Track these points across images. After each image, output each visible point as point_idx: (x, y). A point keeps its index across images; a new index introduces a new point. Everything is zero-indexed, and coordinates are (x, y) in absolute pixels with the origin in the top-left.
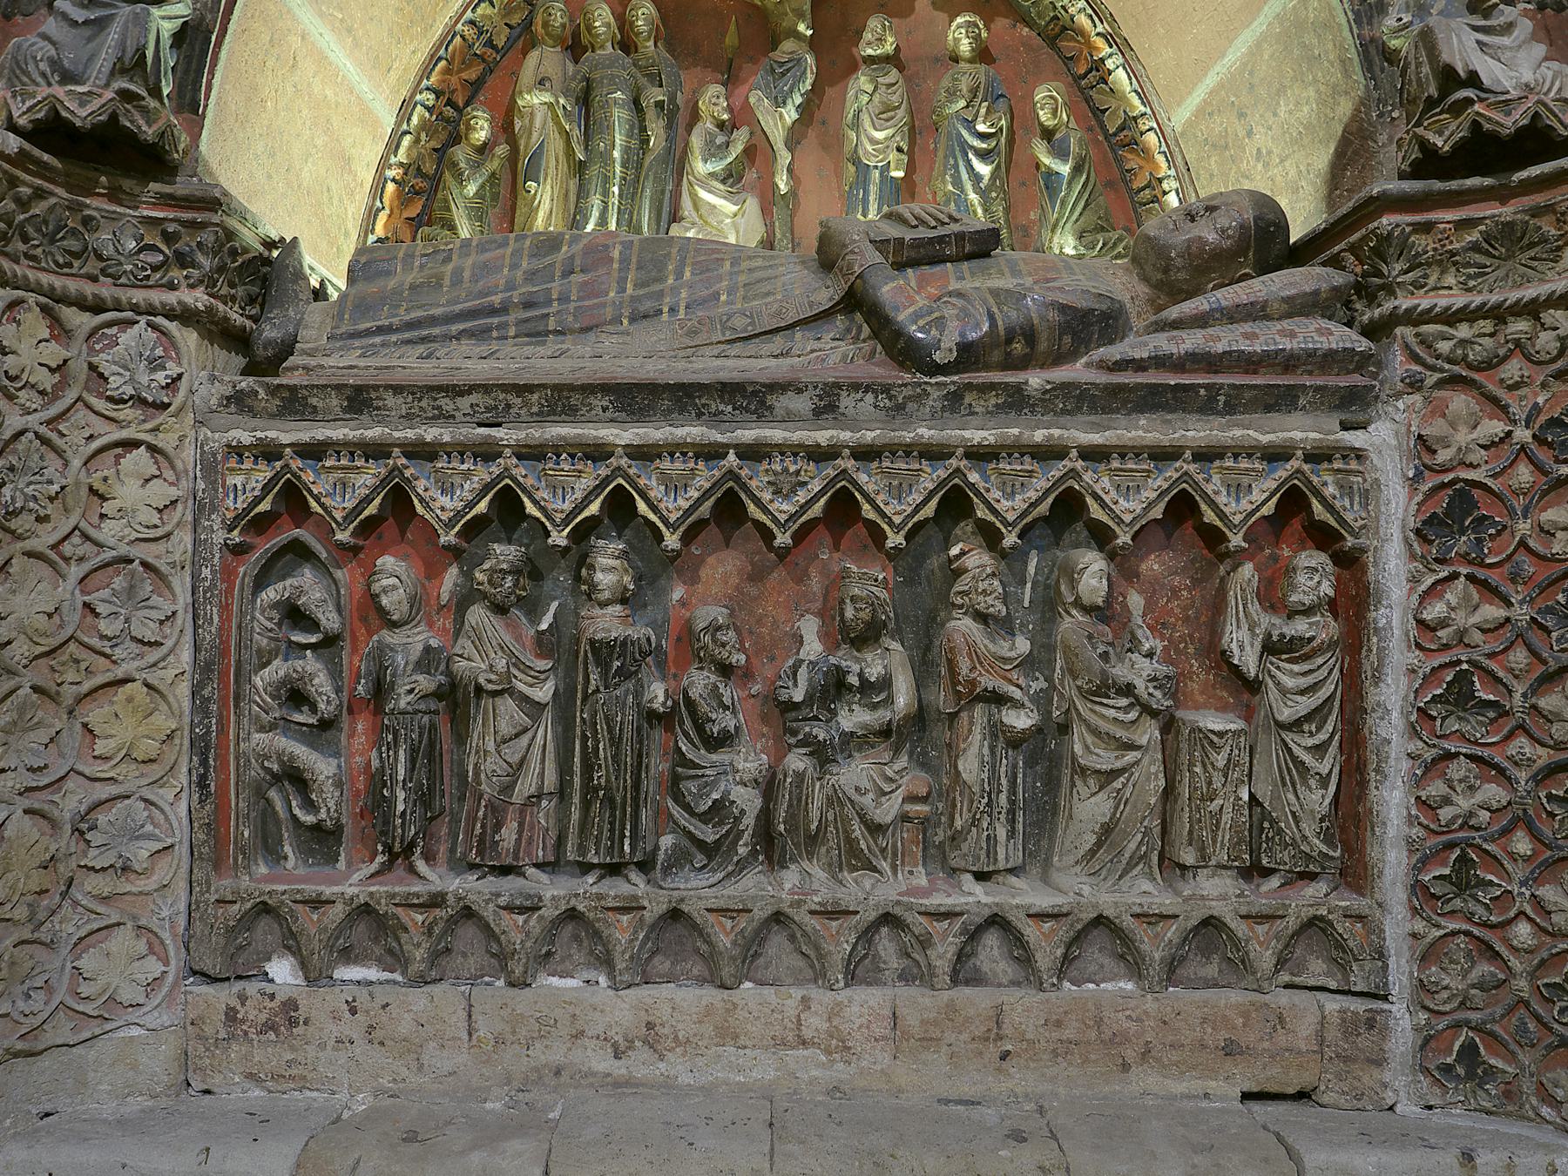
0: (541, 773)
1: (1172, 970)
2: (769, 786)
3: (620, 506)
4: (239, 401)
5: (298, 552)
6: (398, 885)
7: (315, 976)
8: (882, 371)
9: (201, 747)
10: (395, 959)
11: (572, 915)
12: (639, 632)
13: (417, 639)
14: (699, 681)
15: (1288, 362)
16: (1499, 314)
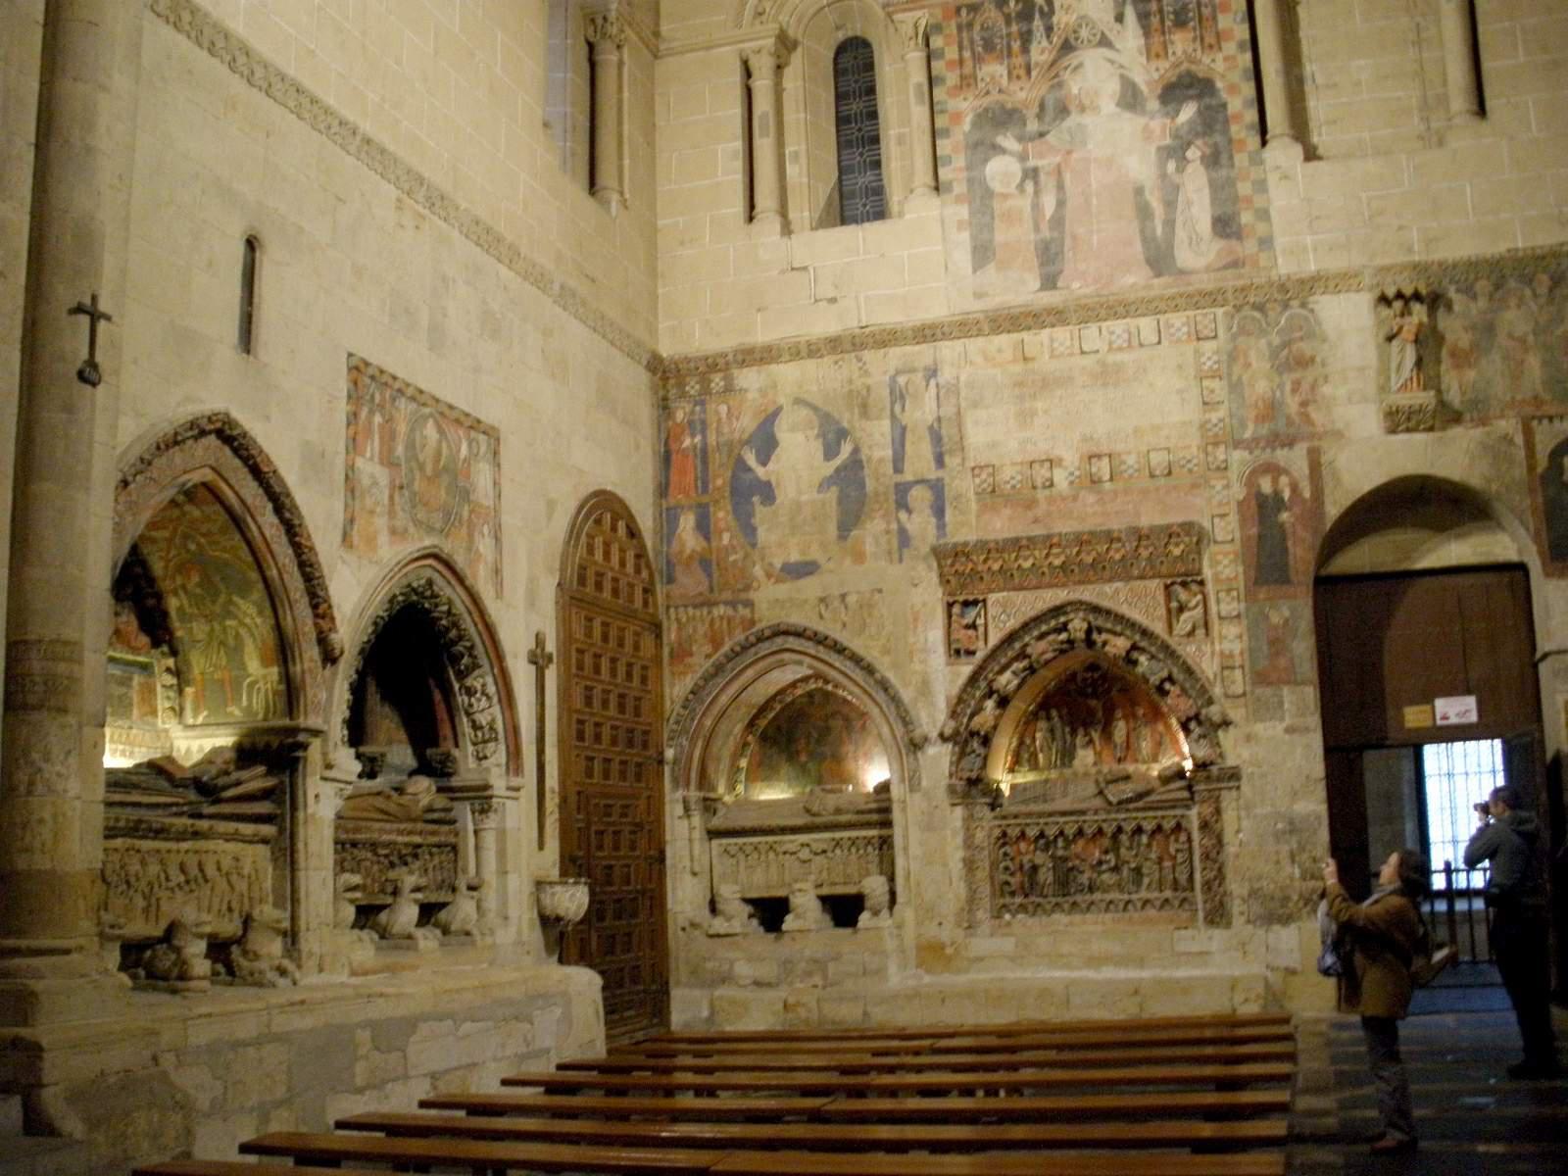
0: (1050, 879)
1: (1162, 907)
2: (1090, 879)
3: (1062, 833)
4: (995, 818)
5: (1004, 844)
6: (1026, 901)
7: (1014, 916)
8: (1104, 805)
9: (992, 878)
10: (1027, 912)
11: (1057, 904)
12: (1066, 853)
13: (1028, 857)
14: (1077, 862)
15: (1177, 800)
16: (1210, 791)
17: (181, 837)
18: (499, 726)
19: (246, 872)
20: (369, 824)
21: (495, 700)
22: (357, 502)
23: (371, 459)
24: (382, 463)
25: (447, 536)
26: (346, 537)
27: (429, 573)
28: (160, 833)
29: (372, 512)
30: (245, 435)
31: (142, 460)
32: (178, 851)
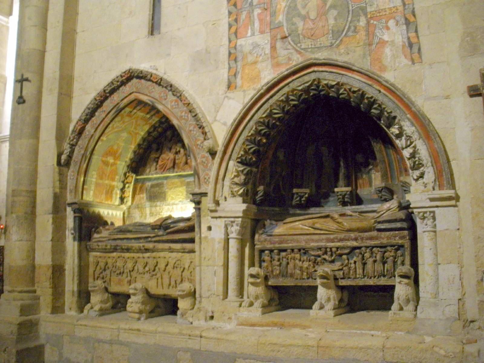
17: (140, 250)
18: (423, 153)
19: (187, 267)
20: (295, 237)
21: (415, 136)
22: (239, 64)
23: (253, 34)
24: (262, 32)
25: (338, 46)
26: (230, 86)
27: (313, 76)
28: (128, 250)
29: (255, 63)
30: (141, 72)
31: (89, 109)
32: (144, 258)
